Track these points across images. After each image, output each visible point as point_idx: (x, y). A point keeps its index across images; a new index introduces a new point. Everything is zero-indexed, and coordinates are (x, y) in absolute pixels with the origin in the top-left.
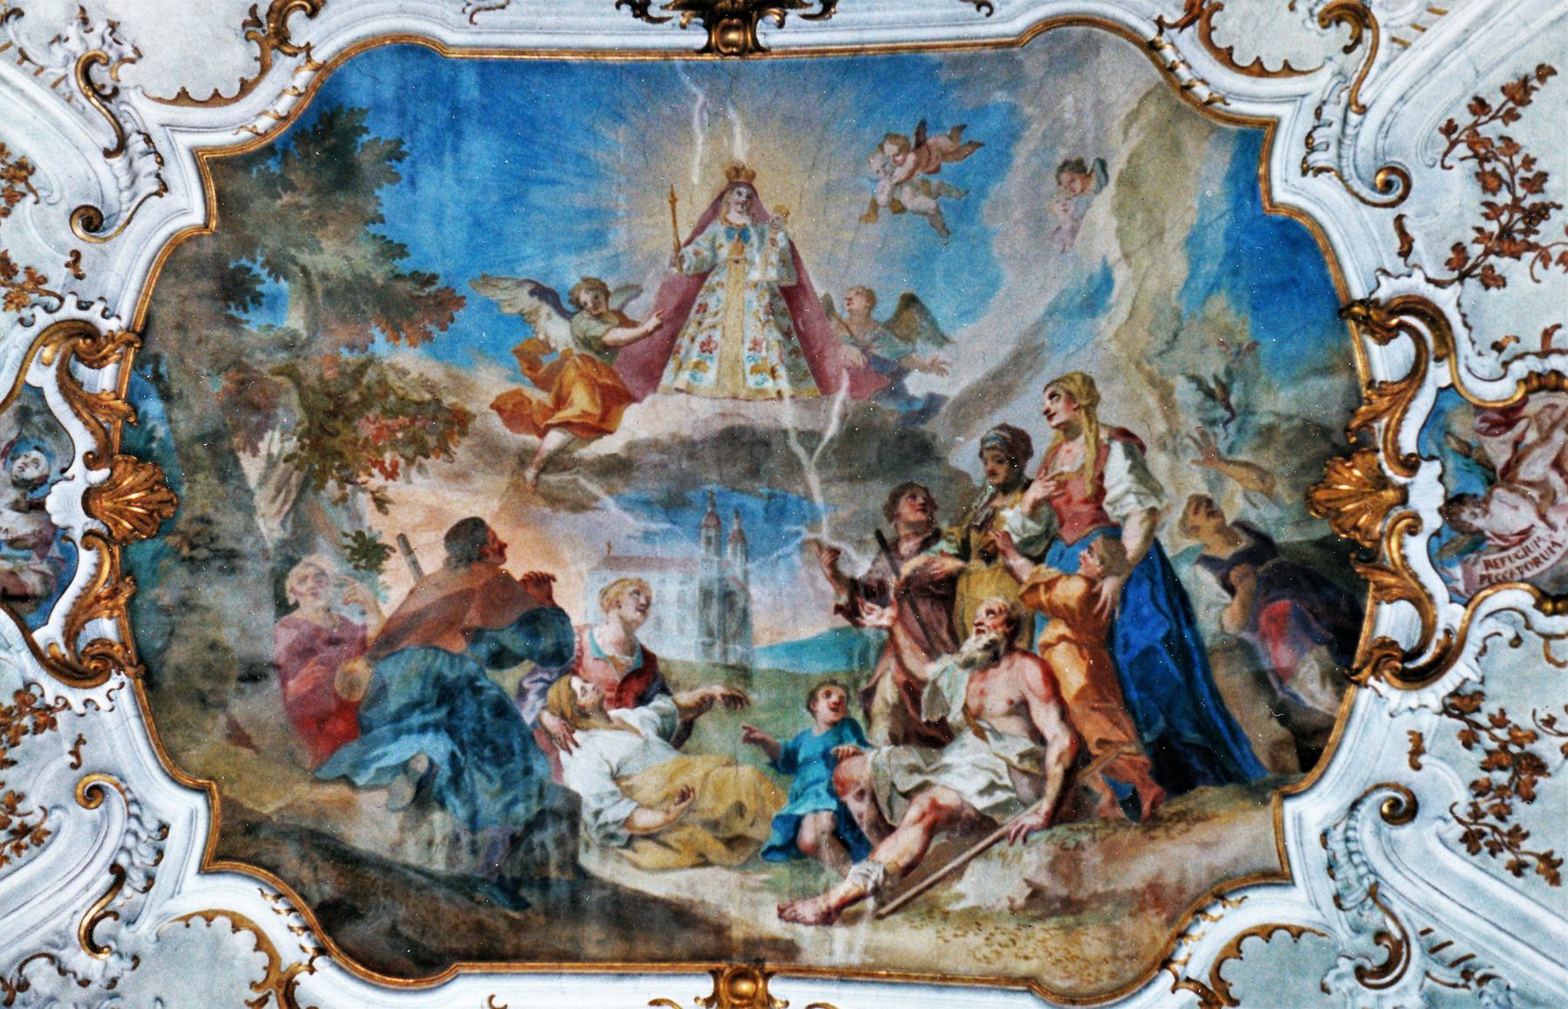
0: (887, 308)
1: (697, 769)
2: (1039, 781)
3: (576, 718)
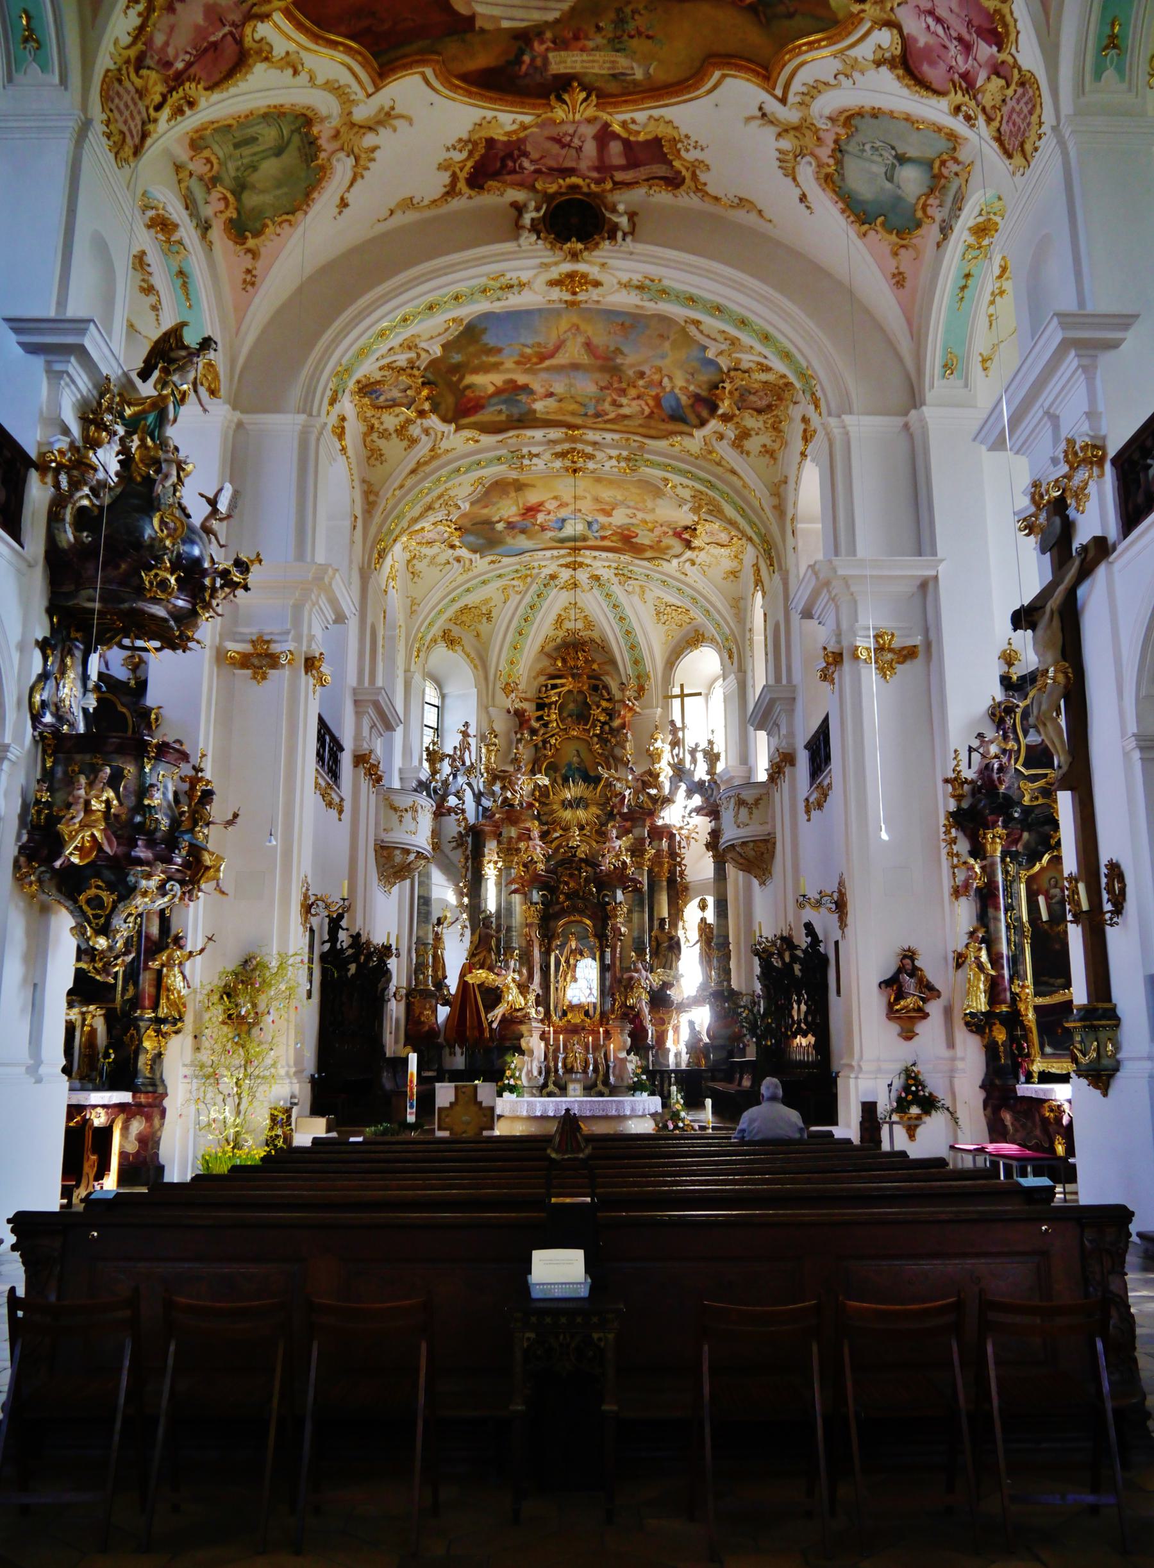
0: (612, 348)
1: (563, 405)
3: (535, 400)
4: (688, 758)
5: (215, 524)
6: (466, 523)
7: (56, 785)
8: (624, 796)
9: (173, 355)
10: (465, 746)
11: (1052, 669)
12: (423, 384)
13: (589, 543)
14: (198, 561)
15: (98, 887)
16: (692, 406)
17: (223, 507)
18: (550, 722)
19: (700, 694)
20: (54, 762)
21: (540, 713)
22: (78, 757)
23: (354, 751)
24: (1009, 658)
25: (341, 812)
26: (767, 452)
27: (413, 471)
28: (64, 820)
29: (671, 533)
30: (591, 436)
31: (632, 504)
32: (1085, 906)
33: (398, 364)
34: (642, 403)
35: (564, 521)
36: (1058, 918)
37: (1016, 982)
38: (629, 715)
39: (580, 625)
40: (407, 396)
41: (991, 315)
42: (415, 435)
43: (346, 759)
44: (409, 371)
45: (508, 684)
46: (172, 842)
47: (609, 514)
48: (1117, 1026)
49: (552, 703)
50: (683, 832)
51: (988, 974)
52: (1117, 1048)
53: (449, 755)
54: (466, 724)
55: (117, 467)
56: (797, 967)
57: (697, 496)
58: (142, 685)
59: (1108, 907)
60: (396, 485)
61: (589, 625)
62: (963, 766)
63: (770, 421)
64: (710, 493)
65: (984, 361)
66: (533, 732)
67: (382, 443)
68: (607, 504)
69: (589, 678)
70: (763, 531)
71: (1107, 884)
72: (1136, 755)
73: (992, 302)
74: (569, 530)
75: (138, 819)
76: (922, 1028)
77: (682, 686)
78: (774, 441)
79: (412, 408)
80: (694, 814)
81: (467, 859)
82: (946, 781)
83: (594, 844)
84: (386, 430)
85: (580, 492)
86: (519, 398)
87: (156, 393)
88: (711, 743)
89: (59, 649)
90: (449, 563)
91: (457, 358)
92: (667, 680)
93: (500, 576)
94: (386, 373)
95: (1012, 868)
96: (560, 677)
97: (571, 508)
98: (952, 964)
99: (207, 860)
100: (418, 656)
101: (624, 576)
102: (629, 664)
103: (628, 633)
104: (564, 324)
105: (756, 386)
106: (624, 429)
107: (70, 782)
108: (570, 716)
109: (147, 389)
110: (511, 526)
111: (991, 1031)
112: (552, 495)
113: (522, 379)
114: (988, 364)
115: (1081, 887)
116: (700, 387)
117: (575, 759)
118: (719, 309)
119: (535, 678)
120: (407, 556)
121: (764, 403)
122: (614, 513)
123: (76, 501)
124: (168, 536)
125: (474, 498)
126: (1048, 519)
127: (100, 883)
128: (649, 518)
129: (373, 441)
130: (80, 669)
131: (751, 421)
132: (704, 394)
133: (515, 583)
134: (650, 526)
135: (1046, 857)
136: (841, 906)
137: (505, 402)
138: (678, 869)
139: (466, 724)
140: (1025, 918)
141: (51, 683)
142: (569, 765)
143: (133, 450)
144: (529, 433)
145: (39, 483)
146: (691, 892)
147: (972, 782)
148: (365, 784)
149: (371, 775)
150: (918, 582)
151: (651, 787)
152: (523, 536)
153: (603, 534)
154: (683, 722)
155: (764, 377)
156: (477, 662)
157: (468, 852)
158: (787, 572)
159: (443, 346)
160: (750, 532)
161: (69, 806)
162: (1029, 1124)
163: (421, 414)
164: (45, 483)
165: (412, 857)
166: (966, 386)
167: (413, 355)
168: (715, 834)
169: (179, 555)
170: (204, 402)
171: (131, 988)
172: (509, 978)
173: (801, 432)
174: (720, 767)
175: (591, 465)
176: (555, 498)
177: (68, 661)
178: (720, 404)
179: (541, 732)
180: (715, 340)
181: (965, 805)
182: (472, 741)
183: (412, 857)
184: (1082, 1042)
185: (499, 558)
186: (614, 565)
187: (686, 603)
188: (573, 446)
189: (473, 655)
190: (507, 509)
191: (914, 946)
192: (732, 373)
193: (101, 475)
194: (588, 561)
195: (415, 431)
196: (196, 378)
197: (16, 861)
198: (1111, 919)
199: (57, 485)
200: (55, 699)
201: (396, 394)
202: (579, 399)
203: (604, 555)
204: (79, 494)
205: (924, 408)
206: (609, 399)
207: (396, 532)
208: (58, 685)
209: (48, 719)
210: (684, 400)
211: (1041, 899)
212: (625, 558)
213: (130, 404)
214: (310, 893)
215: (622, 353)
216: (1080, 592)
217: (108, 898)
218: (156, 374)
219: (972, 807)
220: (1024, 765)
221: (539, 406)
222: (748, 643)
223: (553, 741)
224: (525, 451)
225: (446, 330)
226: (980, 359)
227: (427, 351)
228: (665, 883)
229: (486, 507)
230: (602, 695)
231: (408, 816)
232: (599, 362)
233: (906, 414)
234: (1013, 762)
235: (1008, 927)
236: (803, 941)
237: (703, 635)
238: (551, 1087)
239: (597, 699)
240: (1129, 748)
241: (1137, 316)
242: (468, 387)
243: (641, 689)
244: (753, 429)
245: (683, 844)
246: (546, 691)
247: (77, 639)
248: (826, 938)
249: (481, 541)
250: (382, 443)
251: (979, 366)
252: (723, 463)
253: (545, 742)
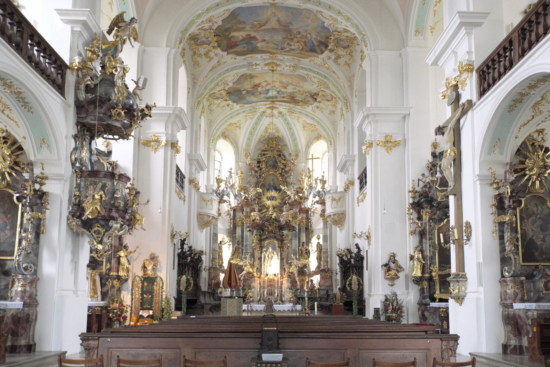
0: (288, 22)
1: (268, 45)
2: (299, 48)
4: (314, 182)
5: (138, 92)
6: (231, 91)
7: (82, 190)
8: (290, 197)
9: (120, 25)
10: (231, 177)
11: (449, 150)
12: (215, 35)
13: (278, 99)
14: (132, 106)
15: (98, 227)
16: (318, 46)
17: (140, 85)
18: (263, 168)
19: (319, 158)
20: (80, 181)
21: (259, 165)
22: (89, 179)
23: (189, 178)
24: (435, 146)
25: (184, 201)
26: (347, 64)
27: (211, 70)
28: (85, 202)
29: (309, 96)
30: (279, 57)
31: (294, 84)
32: (457, 238)
33: (205, 28)
34: (299, 44)
35: (268, 90)
36: (447, 241)
37: (432, 266)
38: (292, 166)
39: (274, 131)
40: (208, 41)
41: (435, 11)
42: (212, 56)
43: (186, 181)
44: (209, 30)
45: (246, 153)
46: (125, 211)
47: (286, 88)
48: (466, 281)
49: (263, 161)
51: (422, 263)
52: (466, 289)
53: (225, 181)
54: (231, 169)
55: (100, 68)
56: (352, 260)
57: (320, 82)
58: (110, 153)
59: (465, 238)
60: (204, 76)
61: (278, 131)
62: (416, 186)
63: (348, 52)
64: (325, 80)
65: (432, 29)
66: (256, 172)
67: (199, 59)
68: (285, 84)
69: (277, 151)
70: (345, 95)
71: (465, 230)
72: (478, 182)
73: (436, 5)
74: (270, 94)
75: (112, 202)
76: (396, 282)
77: (312, 155)
78: (349, 60)
79: (211, 45)
80: (316, 204)
81: (231, 219)
82: (410, 192)
84: (200, 54)
85: (275, 79)
86: (252, 42)
87: (114, 40)
88: (323, 177)
89: (81, 138)
90: (224, 106)
91: (228, 26)
92: (307, 153)
93: (244, 112)
94: (201, 31)
95: (432, 224)
96: (266, 151)
97: (271, 85)
98: (408, 259)
99: (138, 217)
100: (212, 142)
101: (291, 112)
103: (293, 134)
104: (269, 12)
105: (344, 38)
106: (291, 54)
107: (87, 188)
108: (270, 166)
109: (111, 38)
110: (248, 92)
111: (422, 283)
112: (264, 80)
113: (253, 34)
114: (433, 30)
115: (456, 231)
116: (321, 38)
117: (272, 183)
118: (330, 7)
119: (257, 151)
120: (208, 103)
121: (346, 45)
122: (288, 87)
123: (86, 82)
124: (121, 96)
125: (234, 81)
126: (451, 93)
127: (99, 225)
128: (301, 89)
129: (195, 58)
130: (88, 146)
131: (341, 52)
132: (323, 40)
133: (249, 114)
134: (302, 93)
135: (446, 220)
136: (368, 237)
137: (247, 43)
139: (231, 169)
140: (436, 243)
141: (78, 151)
142: (269, 185)
143: (106, 62)
144: (256, 56)
145: (71, 75)
146: (314, 233)
147: (419, 192)
148: (193, 191)
149: (195, 187)
150: (402, 116)
151: (300, 193)
152: (253, 96)
153: (283, 95)
154: (313, 169)
155: (346, 34)
156: (235, 145)
157: (231, 217)
158: (353, 111)
159: (223, 21)
160: (340, 96)
161: (87, 197)
162: (435, 317)
163: (214, 47)
164: (73, 75)
165: (211, 218)
166: (424, 39)
167: (211, 24)
168: (324, 211)
169: (125, 104)
170: (133, 44)
171: (108, 264)
172: (247, 262)
173: (360, 57)
174: (326, 186)
175: (279, 69)
176: (265, 81)
177: (84, 143)
178: (329, 45)
179: (259, 172)
180: (328, 19)
181: (416, 201)
182: (233, 175)
183: (211, 218)
184: (453, 286)
185: (243, 105)
186: (288, 108)
187: (315, 123)
188: (273, 61)
190: (247, 85)
191: (395, 252)
192: (334, 33)
193: (94, 72)
194: (277, 106)
195: (212, 54)
196: (129, 34)
197: (68, 217)
198: (466, 242)
199: (78, 76)
200: (80, 158)
201: (204, 39)
202: (275, 42)
203: (284, 104)
204: (86, 79)
205: (408, 48)
206: (286, 43)
207: (204, 94)
208: (81, 152)
209: (78, 165)
210: (316, 43)
211: (441, 235)
212: (291, 105)
213: (104, 44)
214: (174, 230)
215: (292, 24)
216: (462, 121)
217: (102, 231)
218: (114, 32)
219: (419, 201)
220: (439, 186)
221: (259, 45)
222: (338, 139)
223: (263, 175)
224: (254, 63)
225: (224, 14)
226: (430, 28)
227: (216, 23)
229: (239, 85)
231: (209, 203)
232: (283, 28)
233: (400, 50)
234: (435, 185)
235: (430, 246)
236: (355, 250)
237: (321, 135)
238: (262, 301)
239: (280, 159)
240: (475, 180)
241: (489, 13)
242: (232, 37)
243: (297, 156)
244: (342, 55)
245: (312, 215)
247: (87, 135)
248: (363, 249)
249: (237, 98)
250: (199, 59)
251: (430, 31)
252: (330, 68)
253: (260, 176)
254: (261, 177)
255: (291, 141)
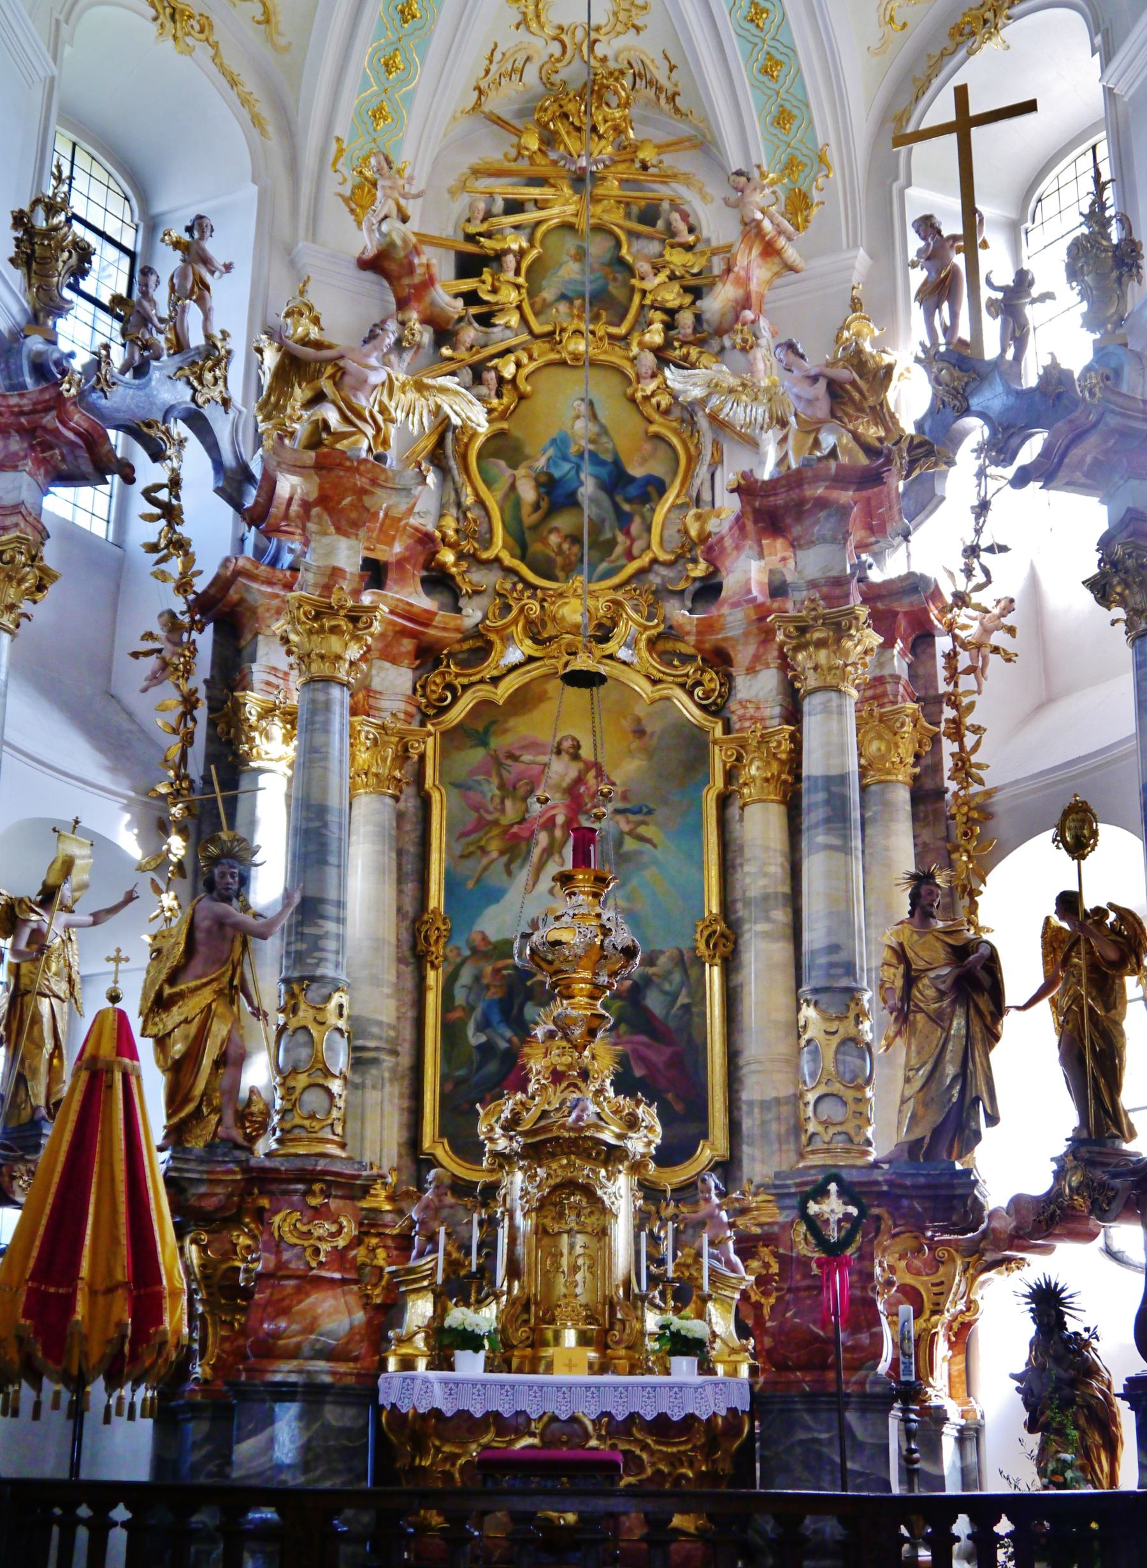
4: (992, 328)
50: (963, 616)
83: (642, 686)
102: (756, 128)
108: (563, 297)
117: (580, 424)
138: (949, 747)
142: (560, 443)
156: (264, 110)
179: (470, 334)
189: (249, 84)
228: (902, 796)
230: (671, 232)
239: (654, 247)
246: (488, 215)
254: (491, 376)
255: (744, 76)
